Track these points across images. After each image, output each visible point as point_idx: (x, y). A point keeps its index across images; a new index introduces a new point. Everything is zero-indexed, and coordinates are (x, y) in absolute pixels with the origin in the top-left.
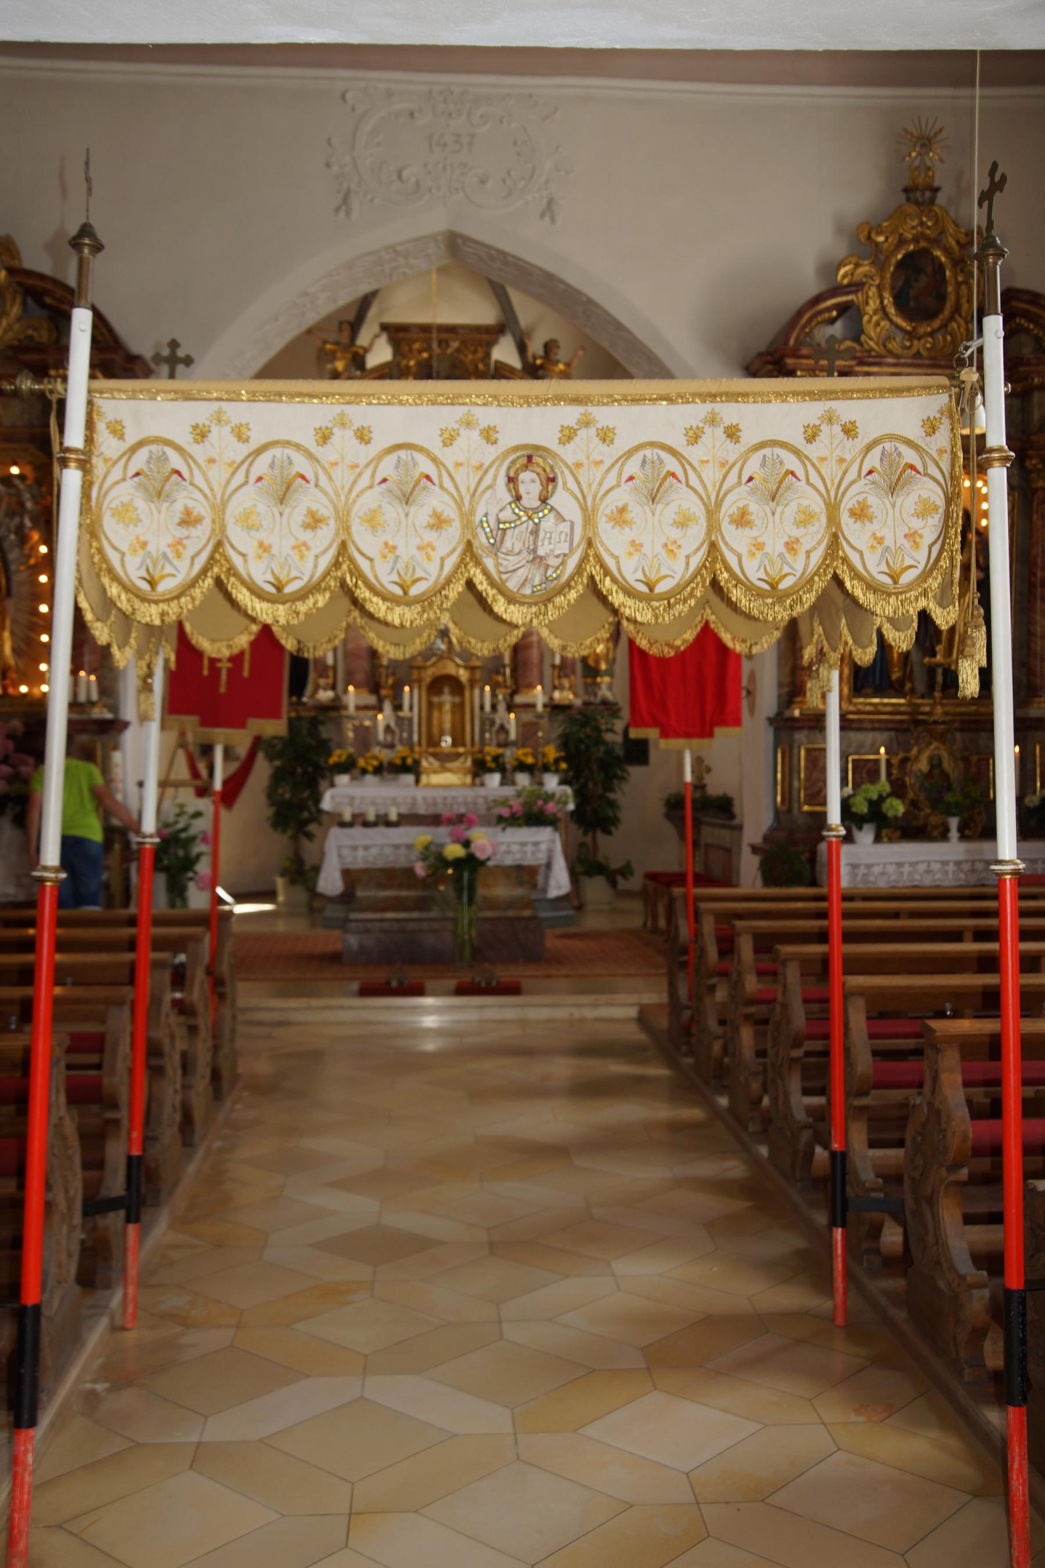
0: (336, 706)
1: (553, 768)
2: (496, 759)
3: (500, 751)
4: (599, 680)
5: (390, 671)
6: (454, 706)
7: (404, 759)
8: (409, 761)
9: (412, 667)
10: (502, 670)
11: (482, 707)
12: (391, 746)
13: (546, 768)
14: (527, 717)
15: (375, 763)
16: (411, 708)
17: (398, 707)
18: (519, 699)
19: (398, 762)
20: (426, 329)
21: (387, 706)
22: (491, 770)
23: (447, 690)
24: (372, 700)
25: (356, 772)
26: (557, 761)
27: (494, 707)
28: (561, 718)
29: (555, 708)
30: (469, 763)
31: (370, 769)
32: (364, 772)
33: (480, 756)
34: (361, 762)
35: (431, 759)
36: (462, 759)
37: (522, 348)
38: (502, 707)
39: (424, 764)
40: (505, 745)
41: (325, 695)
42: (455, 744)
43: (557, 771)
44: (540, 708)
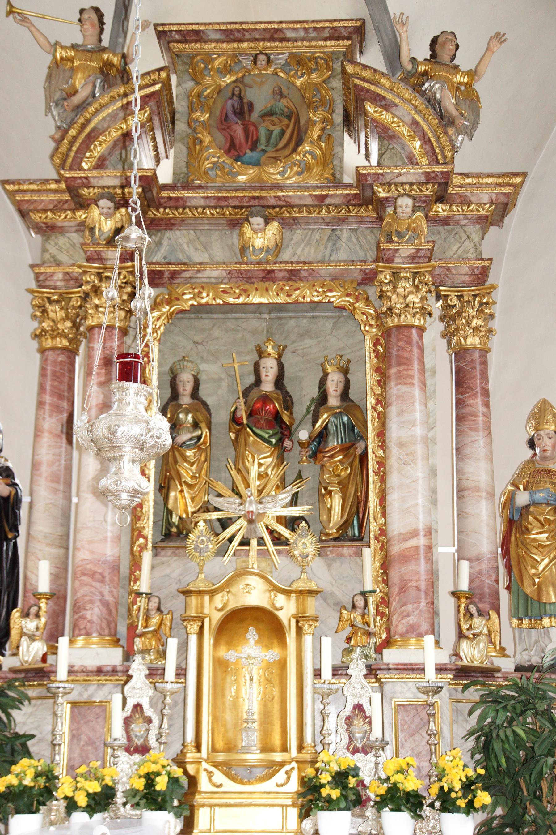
0: (41, 673)
1: (462, 803)
2: (340, 778)
3: (351, 760)
4: (546, 621)
5: (154, 604)
6: (268, 667)
7: (150, 779)
8: (161, 784)
9: (187, 593)
10: (360, 602)
11: (318, 673)
12: (144, 750)
13: (447, 803)
14: (405, 691)
15: (95, 787)
16: (181, 672)
17: (155, 674)
18: (391, 656)
19: (140, 784)
20: (232, 34)
21: (138, 668)
22: (330, 805)
23: (252, 635)
24: (113, 656)
25: (58, 806)
26: (468, 786)
27: (340, 671)
28: (474, 693)
29: (464, 673)
30: (294, 786)
31: (82, 800)
32: (72, 806)
33: (310, 772)
34: (65, 787)
35: (219, 777)
36: (280, 777)
37: (393, 54)
38: (357, 669)
39: (204, 784)
40: (365, 751)
41: (31, 651)
42: (266, 748)
43: (470, 808)
44: (430, 674)
